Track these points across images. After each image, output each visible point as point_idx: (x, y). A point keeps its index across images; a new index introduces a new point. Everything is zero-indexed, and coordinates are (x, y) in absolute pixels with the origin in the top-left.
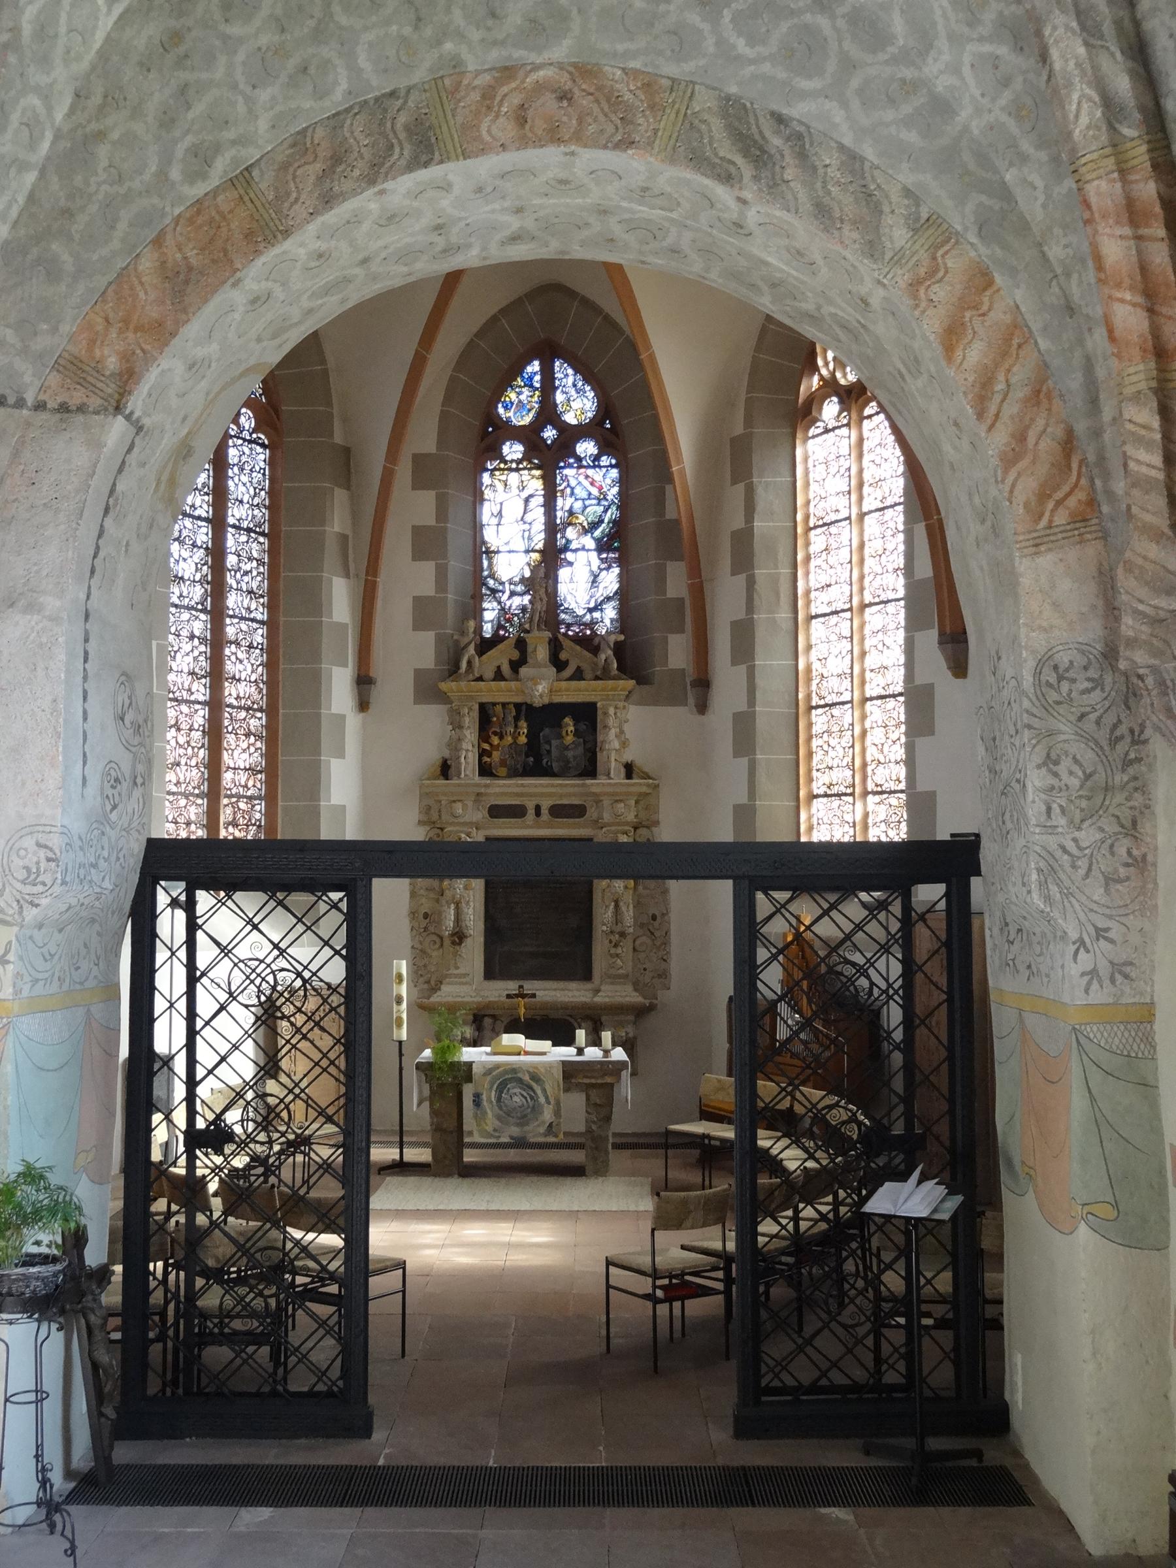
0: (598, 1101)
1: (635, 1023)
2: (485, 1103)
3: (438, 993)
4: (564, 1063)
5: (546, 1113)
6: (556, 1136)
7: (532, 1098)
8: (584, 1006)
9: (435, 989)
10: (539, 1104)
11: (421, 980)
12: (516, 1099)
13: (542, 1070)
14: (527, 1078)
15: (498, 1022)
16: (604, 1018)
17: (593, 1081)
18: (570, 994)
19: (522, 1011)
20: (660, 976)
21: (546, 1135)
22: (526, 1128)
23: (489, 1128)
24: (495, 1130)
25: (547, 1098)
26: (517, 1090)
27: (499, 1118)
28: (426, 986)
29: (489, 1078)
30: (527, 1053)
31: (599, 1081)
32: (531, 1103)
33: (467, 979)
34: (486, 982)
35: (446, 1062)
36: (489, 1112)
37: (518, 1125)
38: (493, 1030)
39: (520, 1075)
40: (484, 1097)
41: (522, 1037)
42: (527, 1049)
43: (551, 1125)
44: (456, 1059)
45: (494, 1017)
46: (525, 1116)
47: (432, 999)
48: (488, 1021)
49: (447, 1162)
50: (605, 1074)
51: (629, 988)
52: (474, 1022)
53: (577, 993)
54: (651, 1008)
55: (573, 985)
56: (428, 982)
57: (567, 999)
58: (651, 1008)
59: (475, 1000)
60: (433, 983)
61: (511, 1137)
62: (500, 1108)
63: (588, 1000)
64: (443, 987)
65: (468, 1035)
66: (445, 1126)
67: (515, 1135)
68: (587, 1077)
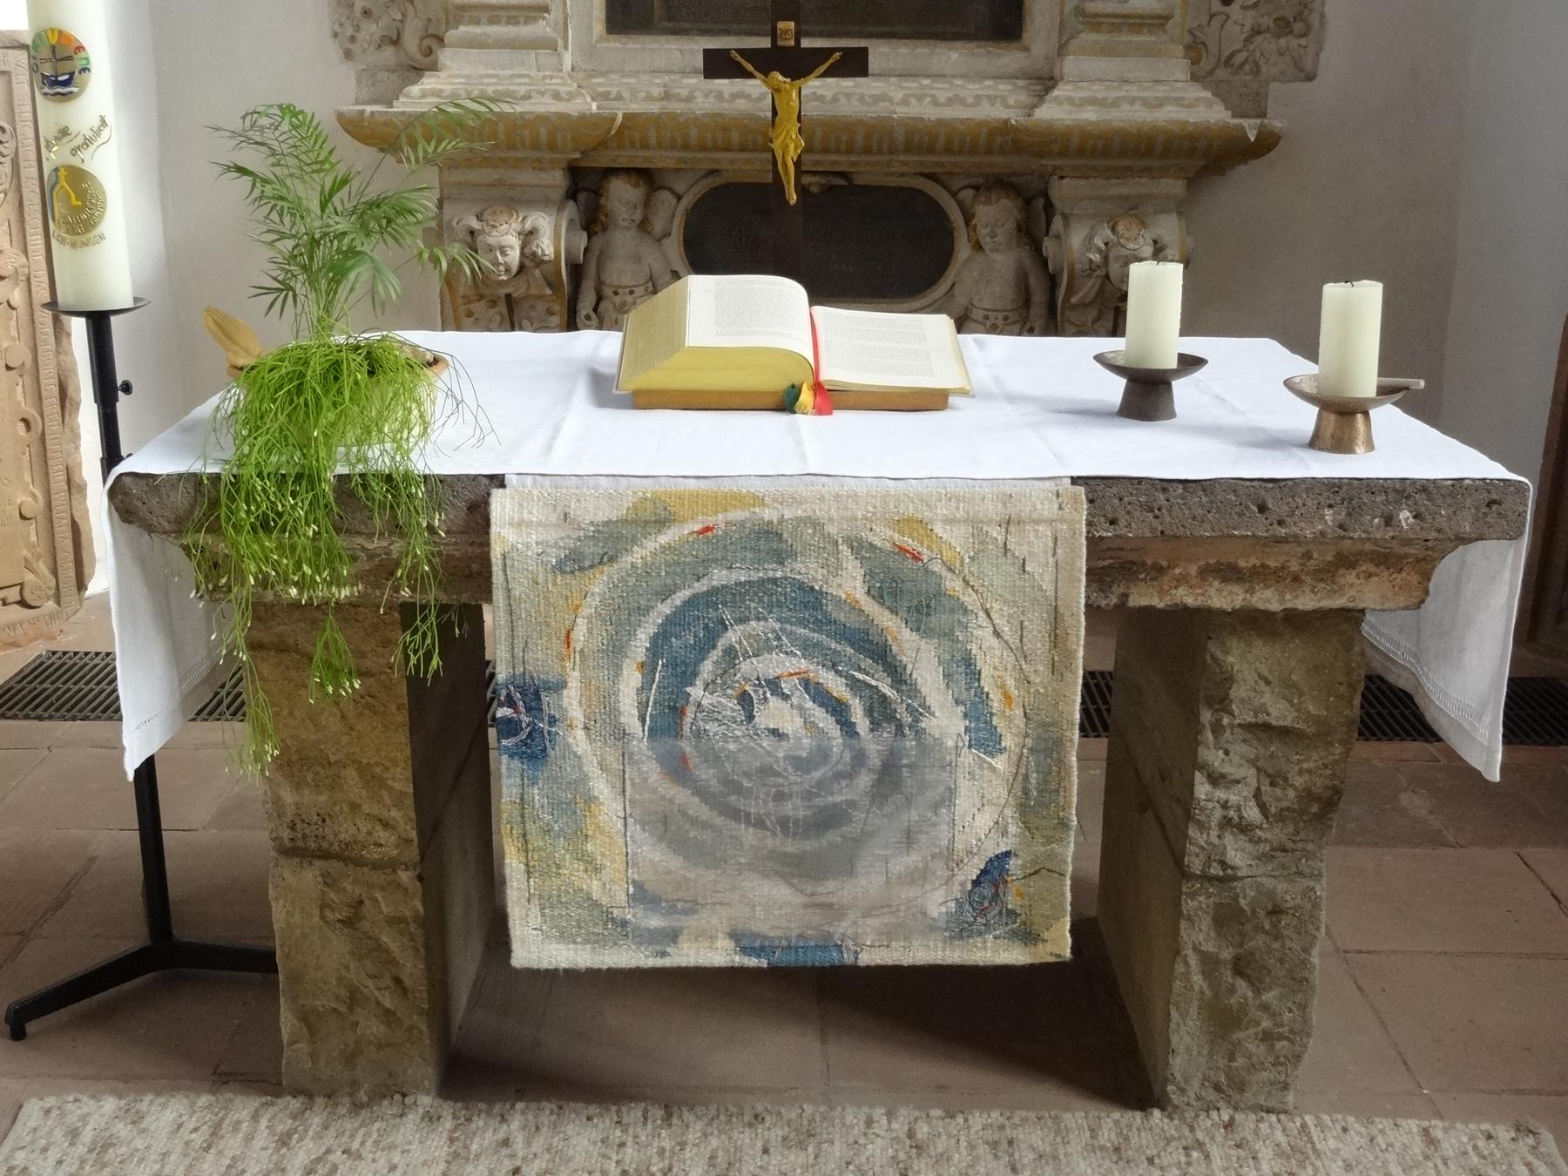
0: (1279, 712)
1: (1181, 208)
2: (579, 741)
3: (429, 82)
4: (1097, 488)
5: (965, 802)
6: (1028, 936)
7: (880, 711)
8: (1004, 138)
9: (416, 70)
10: (928, 748)
11: (371, 30)
12: (773, 713)
13: (955, 538)
14: (850, 584)
15: (665, 198)
16: (1063, 191)
17: (1268, 599)
18: (942, 91)
19: (790, 146)
20: (1284, 26)
21: (960, 930)
22: (831, 889)
23: (611, 888)
24: (642, 896)
25: (977, 711)
26: (786, 664)
27: (664, 825)
28: (389, 53)
29: (598, 584)
30: (831, 398)
31: (1306, 602)
32: (874, 745)
33: (542, 28)
34: (616, 44)
35: (306, 478)
36: (601, 787)
37: (797, 869)
38: (644, 225)
39: (808, 570)
40: (572, 702)
41: (791, 291)
42: (831, 374)
43: (994, 872)
44: (379, 457)
45: (648, 178)
46: (828, 820)
47: (401, 106)
48: (622, 196)
49: (373, 1028)
50: (1346, 561)
51: (1178, 68)
52: (571, 195)
53: (971, 89)
54: (1266, 144)
55: (951, 56)
56: (396, 42)
57: (928, 112)
58: (1266, 144)
59: (573, 108)
60: (411, 43)
61: (740, 939)
62: (678, 769)
63: (1013, 116)
64: (445, 56)
65: (546, 246)
66: (346, 830)
67: (765, 925)
68: (1229, 573)
